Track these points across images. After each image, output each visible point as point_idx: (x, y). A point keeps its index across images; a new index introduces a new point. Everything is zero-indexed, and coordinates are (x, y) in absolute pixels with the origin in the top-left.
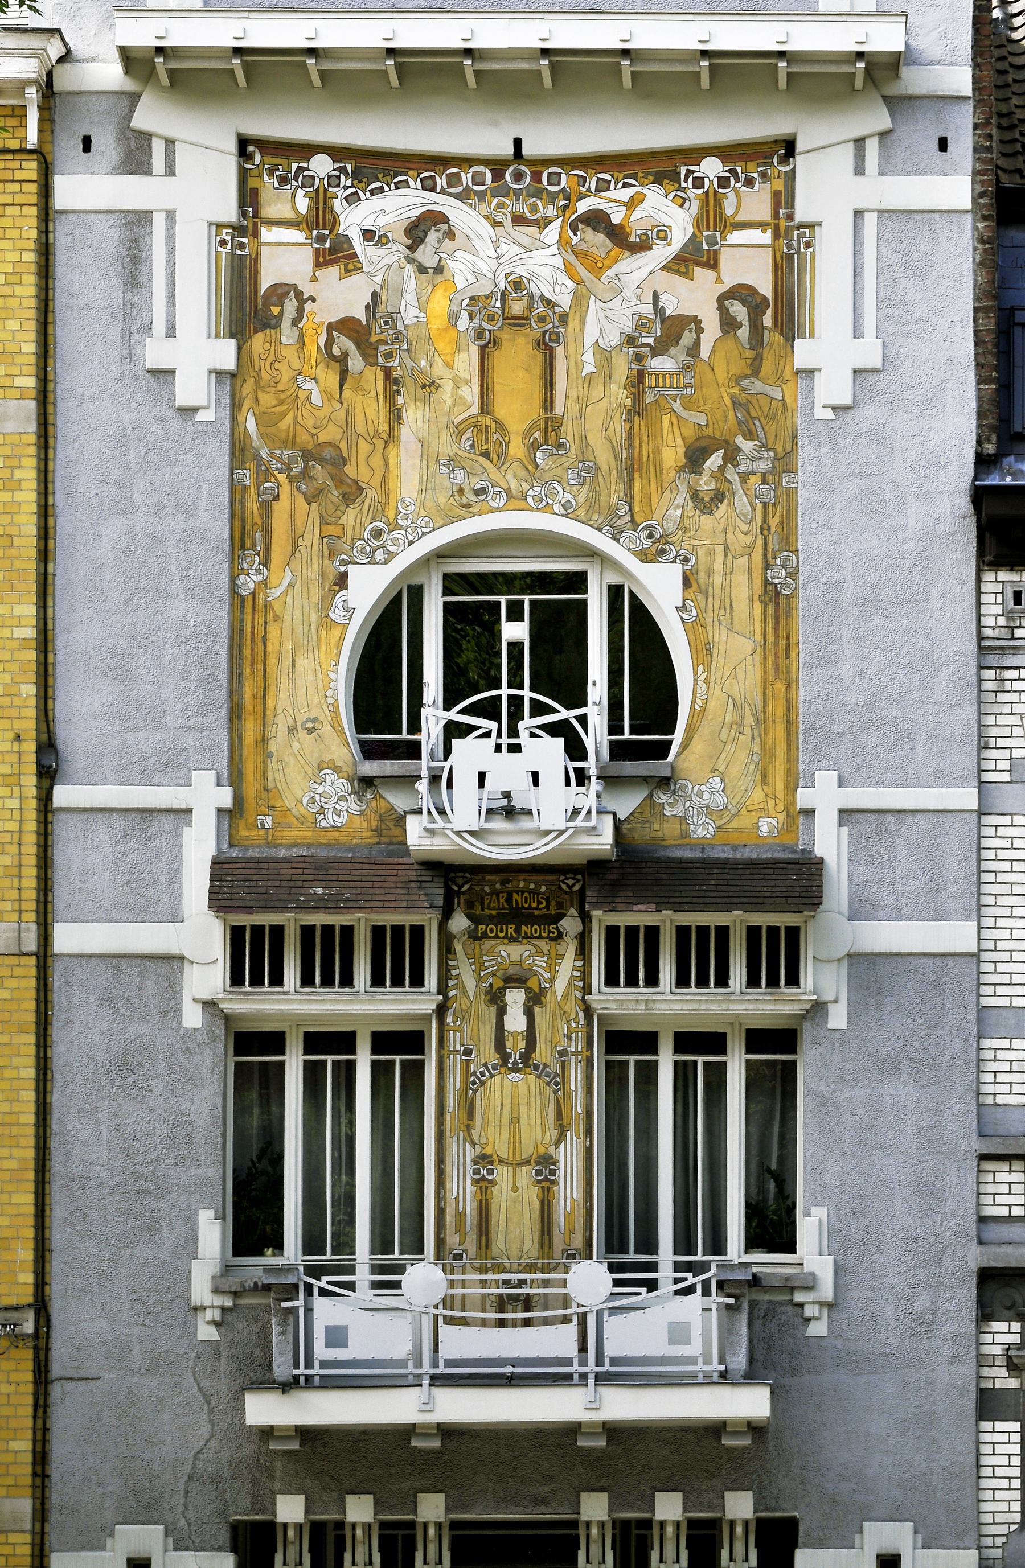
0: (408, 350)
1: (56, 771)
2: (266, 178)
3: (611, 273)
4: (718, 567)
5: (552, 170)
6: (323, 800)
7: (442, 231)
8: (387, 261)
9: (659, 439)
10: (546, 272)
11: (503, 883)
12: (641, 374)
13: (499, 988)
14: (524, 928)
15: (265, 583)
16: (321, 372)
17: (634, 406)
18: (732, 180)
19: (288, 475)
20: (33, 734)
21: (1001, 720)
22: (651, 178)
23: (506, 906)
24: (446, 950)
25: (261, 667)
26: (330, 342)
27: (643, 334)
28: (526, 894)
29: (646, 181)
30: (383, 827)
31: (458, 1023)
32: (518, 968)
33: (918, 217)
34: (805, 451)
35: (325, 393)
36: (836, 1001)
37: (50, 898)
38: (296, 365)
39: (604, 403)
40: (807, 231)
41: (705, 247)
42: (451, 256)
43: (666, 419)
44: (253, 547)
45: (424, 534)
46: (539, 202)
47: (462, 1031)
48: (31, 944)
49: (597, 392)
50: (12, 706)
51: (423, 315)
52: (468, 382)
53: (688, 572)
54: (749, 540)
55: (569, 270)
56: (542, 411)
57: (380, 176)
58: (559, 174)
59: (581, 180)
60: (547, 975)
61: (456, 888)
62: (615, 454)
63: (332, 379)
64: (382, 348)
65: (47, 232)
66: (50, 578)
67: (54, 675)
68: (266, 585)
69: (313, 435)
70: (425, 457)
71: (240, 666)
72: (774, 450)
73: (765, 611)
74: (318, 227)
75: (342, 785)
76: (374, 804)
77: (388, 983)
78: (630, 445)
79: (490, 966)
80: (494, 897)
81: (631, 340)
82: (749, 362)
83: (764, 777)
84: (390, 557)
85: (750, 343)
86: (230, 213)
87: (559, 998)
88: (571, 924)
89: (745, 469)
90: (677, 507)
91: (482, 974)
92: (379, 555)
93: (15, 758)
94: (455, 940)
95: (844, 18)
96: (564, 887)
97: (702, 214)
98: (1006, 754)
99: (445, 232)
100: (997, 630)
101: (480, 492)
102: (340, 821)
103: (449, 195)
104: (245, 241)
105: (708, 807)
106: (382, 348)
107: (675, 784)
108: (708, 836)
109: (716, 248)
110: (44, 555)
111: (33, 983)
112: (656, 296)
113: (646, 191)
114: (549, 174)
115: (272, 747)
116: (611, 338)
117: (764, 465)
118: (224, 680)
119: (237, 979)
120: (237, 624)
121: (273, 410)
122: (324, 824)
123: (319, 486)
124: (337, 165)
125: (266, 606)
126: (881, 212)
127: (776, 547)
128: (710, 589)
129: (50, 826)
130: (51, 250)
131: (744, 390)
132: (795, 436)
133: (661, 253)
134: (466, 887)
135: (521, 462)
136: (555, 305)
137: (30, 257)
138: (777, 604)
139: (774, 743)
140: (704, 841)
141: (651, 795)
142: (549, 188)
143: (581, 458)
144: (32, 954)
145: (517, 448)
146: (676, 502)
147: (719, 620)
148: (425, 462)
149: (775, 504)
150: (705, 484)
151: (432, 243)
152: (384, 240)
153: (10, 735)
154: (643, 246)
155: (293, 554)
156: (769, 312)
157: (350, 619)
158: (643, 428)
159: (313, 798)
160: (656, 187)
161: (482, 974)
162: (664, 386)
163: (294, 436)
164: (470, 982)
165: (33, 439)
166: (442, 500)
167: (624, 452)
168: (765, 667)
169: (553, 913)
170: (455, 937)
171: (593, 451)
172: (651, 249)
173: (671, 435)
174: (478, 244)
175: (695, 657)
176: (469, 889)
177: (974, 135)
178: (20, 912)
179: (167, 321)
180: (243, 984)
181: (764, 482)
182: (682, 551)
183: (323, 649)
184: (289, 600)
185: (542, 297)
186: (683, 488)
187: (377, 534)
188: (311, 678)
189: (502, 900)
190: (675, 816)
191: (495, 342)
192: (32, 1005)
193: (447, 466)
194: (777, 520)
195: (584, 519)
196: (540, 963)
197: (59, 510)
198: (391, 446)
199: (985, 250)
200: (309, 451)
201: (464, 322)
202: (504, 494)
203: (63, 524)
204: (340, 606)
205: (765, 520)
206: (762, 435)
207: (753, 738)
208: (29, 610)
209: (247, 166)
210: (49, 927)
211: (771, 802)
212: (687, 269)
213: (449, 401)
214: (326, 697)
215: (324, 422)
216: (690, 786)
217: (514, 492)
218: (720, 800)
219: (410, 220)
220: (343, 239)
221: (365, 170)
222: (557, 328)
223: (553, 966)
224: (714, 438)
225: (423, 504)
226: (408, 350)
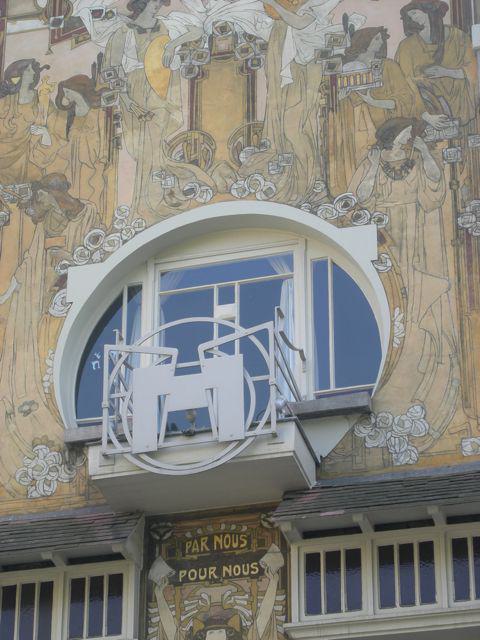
0: (127, 92)
6: (35, 473)
8: (111, 29)
9: (352, 127)
12: (334, 79)
13: (200, 631)
14: (225, 568)
17: (328, 104)
23: (207, 549)
24: (146, 598)
28: (228, 536)
35: (56, 136)
43: (357, 110)
45: (136, 233)
49: (294, 98)
54: (438, 195)
56: (245, 120)
60: (248, 613)
61: (158, 538)
63: (62, 123)
70: (140, 172)
73: (458, 253)
74: (54, 15)
75: (55, 457)
78: (325, 135)
80: (196, 541)
81: (324, 54)
82: (432, 53)
84: (106, 255)
88: (272, 560)
89: (431, 138)
90: (370, 178)
92: (97, 256)
96: (265, 524)
102: (49, 491)
108: (411, 462)
112: (345, 18)
116: (306, 55)
117: (452, 133)
122: (35, 494)
127: (466, 198)
128: (404, 241)
134: (168, 535)
135: (227, 163)
136: (256, 38)
138: (469, 245)
141: (352, 430)
145: (223, 153)
147: (413, 266)
148: (139, 176)
149: (462, 162)
150: (396, 155)
156: (448, 14)
158: (337, 120)
162: (355, 84)
163: (26, 173)
166: (154, 204)
168: (460, 301)
176: (170, 538)
183: (42, 340)
184: (14, 305)
185: (245, 34)
186: (375, 161)
187: (95, 239)
189: (203, 544)
191: (203, 74)
194: (465, 175)
196: (241, 601)
200: (37, 182)
201: (176, 64)
204: (59, 303)
205: (453, 177)
206: (447, 109)
207: (452, 366)
214: (43, 381)
216: (391, 417)
217: (220, 188)
218: (422, 427)
222: (258, 55)
224: (402, 118)
225: (137, 209)
226: (127, 92)
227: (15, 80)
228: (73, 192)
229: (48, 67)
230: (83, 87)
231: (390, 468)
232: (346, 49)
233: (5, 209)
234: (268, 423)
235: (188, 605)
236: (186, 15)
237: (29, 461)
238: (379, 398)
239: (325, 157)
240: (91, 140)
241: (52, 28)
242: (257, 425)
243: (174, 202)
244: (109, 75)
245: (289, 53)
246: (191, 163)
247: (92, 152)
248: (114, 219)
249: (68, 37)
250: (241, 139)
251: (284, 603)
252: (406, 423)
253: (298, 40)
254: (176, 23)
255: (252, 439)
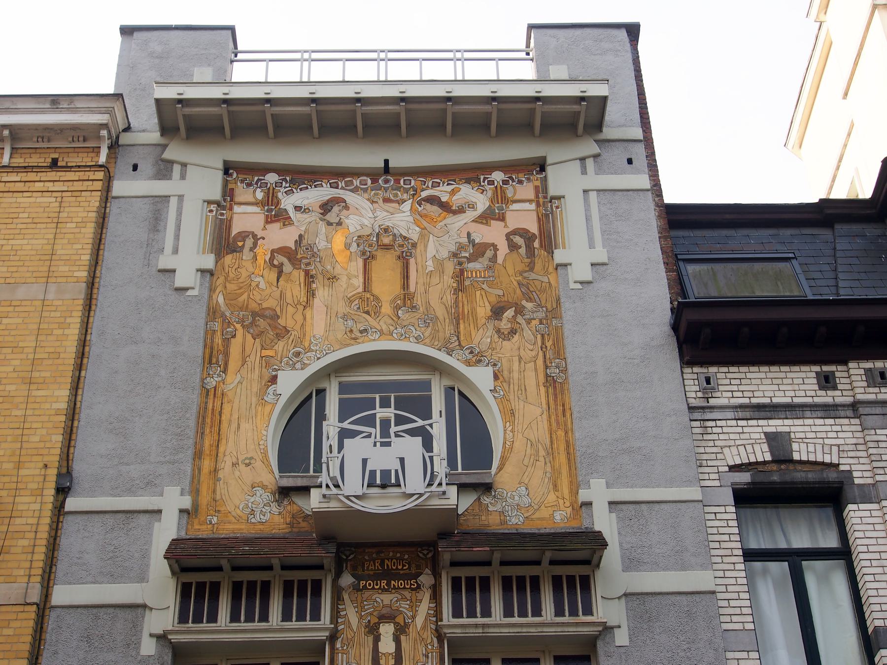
0: (320, 262)
1: (69, 488)
2: (239, 184)
3: (442, 224)
4: (516, 366)
5: (405, 178)
6: (253, 506)
7: (341, 206)
8: (308, 220)
10: (403, 224)
11: (378, 553)
12: (462, 271)
14: (393, 582)
15: (223, 381)
16: (266, 273)
18: (510, 181)
19: (242, 324)
20: (57, 464)
21: (708, 450)
22: (464, 181)
24: (337, 598)
25: (217, 429)
26: (272, 258)
27: (462, 252)
29: (461, 183)
30: (295, 521)
31: (345, 648)
32: (389, 609)
33: (620, 193)
34: (566, 305)
35: (270, 284)
36: (619, 627)
37: (53, 570)
38: (251, 269)
39: (440, 286)
40: (556, 201)
41: (497, 211)
42: (347, 217)
43: (478, 293)
44: (217, 363)
45: (327, 354)
46: (398, 192)
47: (347, 653)
48: (35, 596)
49: (435, 280)
50: (45, 448)
51: (329, 244)
52: (357, 277)
53: (496, 371)
54: (534, 353)
55: (416, 222)
57: (306, 182)
58: (410, 180)
59: (423, 183)
60: (410, 614)
61: (345, 557)
62: (447, 311)
63: (273, 276)
64: (303, 261)
65: (105, 207)
66: (82, 379)
67: (76, 433)
68: (224, 383)
69: (259, 304)
70: (329, 314)
71: (203, 428)
72: (546, 307)
74: (268, 205)
75: (267, 496)
76: (289, 508)
77: (294, 618)
79: (369, 609)
80: (372, 562)
81: (455, 255)
82: (527, 264)
83: (555, 486)
85: (527, 256)
86: (217, 195)
87: (419, 630)
88: (426, 579)
89: (528, 317)
90: (488, 337)
91: (363, 614)
92: (298, 366)
93: (42, 479)
94: (344, 591)
95: (573, 82)
96: (421, 555)
97: (494, 197)
98: (715, 470)
99: (343, 207)
100: (698, 399)
101: (364, 331)
102: (264, 519)
103: (346, 190)
104: (224, 212)
105: (518, 505)
106: (303, 261)
107: (495, 492)
108: (519, 523)
109: (503, 211)
110: (79, 366)
111: (31, 623)
112: (469, 234)
113: (461, 186)
114: (404, 180)
115: (221, 475)
116: (443, 254)
117: (541, 315)
118: (191, 433)
119: (183, 618)
120: (203, 405)
121: (235, 292)
122: (253, 520)
123: (261, 330)
124: (280, 178)
125: (223, 395)
126: (598, 191)
127: (552, 357)
128: (511, 380)
129: (60, 524)
130: (107, 215)
131: (525, 278)
132: (558, 300)
133: (471, 215)
134: (352, 556)
136: (409, 239)
137: (94, 215)
138: (555, 387)
139: (560, 466)
140: (517, 527)
141: (479, 499)
142: (404, 186)
143: (426, 313)
144: (34, 604)
145: (386, 309)
146: (487, 334)
148: (329, 317)
149: (549, 334)
150: (504, 325)
151: (336, 211)
152: (307, 211)
153: (41, 465)
154: (461, 210)
155: (243, 365)
157: (277, 401)
158: (464, 298)
159: (247, 505)
160: (465, 185)
161: (363, 614)
162: (476, 276)
163: (247, 305)
164: (354, 619)
165: (81, 302)
166: (339, 336)
167: (453, 309)
168: (550, 422)
169: (413, 572)
170: (344, 589)
171: (434, 310)
172: (465, 212)
173: (481, 300)
174: (363, 212)
175: (504, 417)
177: (647, 160)
178: (30, 576)
179: (173, 247)
180: (188, 622)
181: (541, 323)
182: (492, 360)
183: (259, 418)
184: (238, 390)
187: (298, 354)
188: (250, 434)
190: (496, 511)
191: (373, 257)
192: (29, 639)
193: (343, 318)
194: (551, 342)
195: (429, 345)
196: (404, 606)
197: (92, 343)
198: (308, 309)
199: (661, 210)
202: (379, 333)
203: (95, 349)
205: (543, 343)
206: (537, 300)
207: (546, 463)
208: (64, 393)
209: (228, 179)
210: (50, 589)
211: (561, 502)
212: (487, 222)
213: (345, 286)
214: (259, 445)
215: (267, 297)
216: (505, 492)
217: (385, 332)
218: (526, 501)
219: (322, 202)
220: (283, 210)
221: (296, 180)
223: (414, 608)
226: (320, 262)
227: (240, 244)
228: (282, 322)
229: (264, 238)
230: (288, 255)
231: (505, 525)
232: (470, 254)
233: (232, 327)
234: (440, 484)
235: (367, 605)
236: (360, 218)
237: (250, 497)
238: (498, 479)
239: (457, 319)
240: (295, 288)
241: (267, 214)
242: (432, 485)
243: (354, 337)
244: (307, 249)
245: (431, 251)
246: (364, 312)
247: (295, 297)
248: (311, 343)
249: (278, 221)
250: (399, 302)
251: (435, 609)
252: (516, 497)
253: (437, 244)
254: (354, 222)
255: (427, 495)
